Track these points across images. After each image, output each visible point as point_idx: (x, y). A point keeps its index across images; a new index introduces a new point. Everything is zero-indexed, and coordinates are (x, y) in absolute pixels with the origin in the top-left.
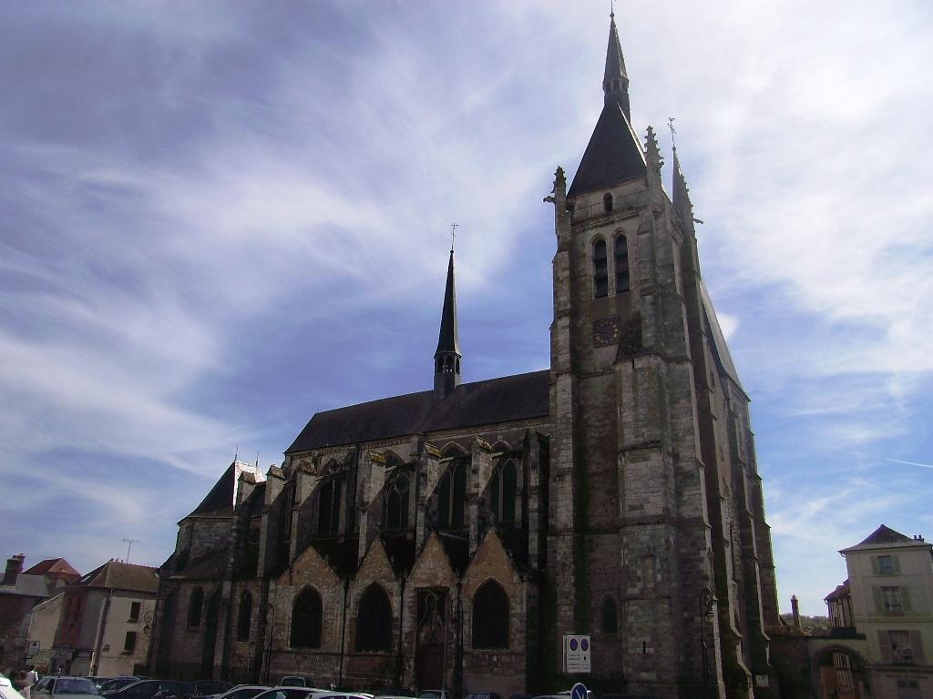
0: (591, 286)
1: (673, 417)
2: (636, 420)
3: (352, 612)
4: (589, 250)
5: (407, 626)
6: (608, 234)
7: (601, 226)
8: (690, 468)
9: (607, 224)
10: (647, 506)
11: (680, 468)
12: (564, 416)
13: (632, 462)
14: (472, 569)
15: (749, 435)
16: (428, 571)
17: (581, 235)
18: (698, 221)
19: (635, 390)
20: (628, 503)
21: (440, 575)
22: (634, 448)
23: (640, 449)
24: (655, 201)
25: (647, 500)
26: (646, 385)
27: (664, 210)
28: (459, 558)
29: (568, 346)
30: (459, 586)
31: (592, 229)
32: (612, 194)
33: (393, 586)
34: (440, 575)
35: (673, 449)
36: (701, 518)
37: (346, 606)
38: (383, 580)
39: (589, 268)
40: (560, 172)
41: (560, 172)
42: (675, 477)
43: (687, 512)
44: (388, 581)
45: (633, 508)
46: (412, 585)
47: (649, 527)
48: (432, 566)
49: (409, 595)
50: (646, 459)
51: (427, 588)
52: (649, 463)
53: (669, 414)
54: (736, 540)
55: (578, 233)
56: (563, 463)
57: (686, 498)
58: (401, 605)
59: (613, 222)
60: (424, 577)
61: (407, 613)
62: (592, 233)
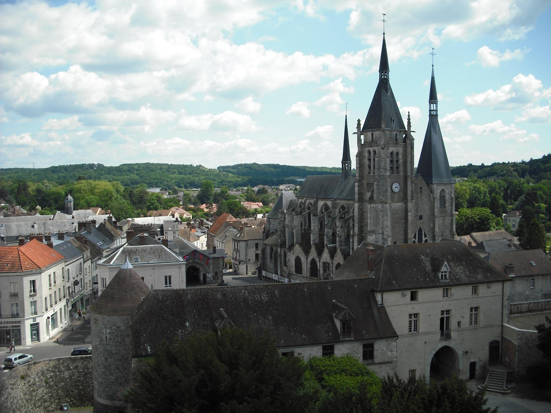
0: (367, 168)
1: (383, 221)
3: (309, 266)
4: (366, 154)
5: (321, 272)
6: (371, 149)
14: (335, 258)
28: (332, 254)
30: (332, 263)
33: (317, 260)
37: (307, 263)
39: (366, 162)
40: (359, 121)
41: (359, 121)
46: (322, 260)
48: (326, 256)
49: (321, 263)
58: (320, 266)
61: (321, 268)
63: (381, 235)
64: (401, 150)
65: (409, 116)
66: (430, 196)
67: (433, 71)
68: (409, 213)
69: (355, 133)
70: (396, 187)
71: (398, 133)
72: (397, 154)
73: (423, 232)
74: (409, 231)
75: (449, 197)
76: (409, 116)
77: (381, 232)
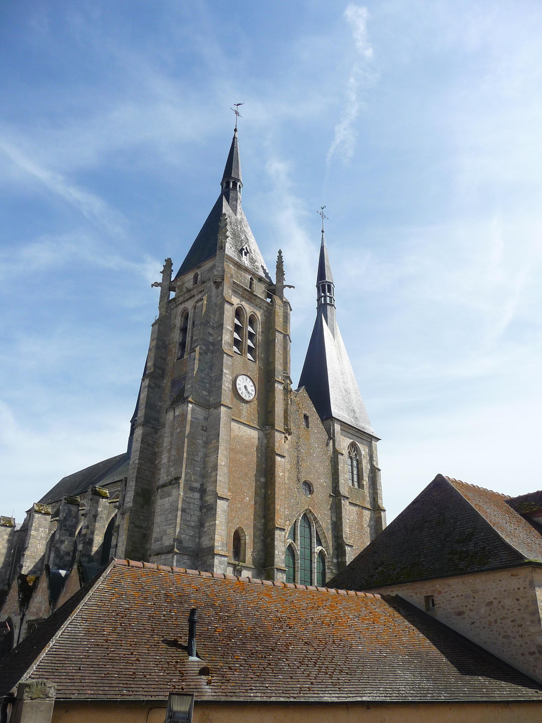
0: (176, 350)
2: (169, 462)
7: (187, 300)
8: (212, 501)
9: (191, 298)
10: (165, 538)
11: (206, 501)
12: (134, 462)
13: (161, 498)
15: (374, 471)
16: (37, 605)
17: (175, 310)
18: (290, 287)
19: (172, 435)
20: (154, 535)
21: (43, 608)
22: (164, 486)
23: (167, 486)
24: (215, 273)
25: (165, 533)
26: (178, 430)
27: (223, 280)
29: (145, 403)
31: (181, 303)
32: (199, 273)
33: (16, 620)
34: (43, 608)
35: (202, 485)
36: (212, 548)
38: (13, 615)
39: (176, 336)
40: (169, 263)
42: (201, 510)
43: (205, 542)
44: (15, 615)
45: (157, 540)
47: (163, 557)
49: (25, 626)
50: (169, 496)
51: (33, 621)
52: (171, 498)
53: (201, 454)
54: (329, 568)
55: (173, 309)
56: (128, 502)
57: (206, 529)
59: (194, 296)
60: (35, 610)
62: (181, 307)
63: (197, 495)
64: (259, 315)
65: (280, 258)
66: (327, 444)
67: (322, 239)
68: (278, 459)
69: (156, 284)
70: (247, 387)
71: (255, 281)
72: (252, 321)
73: (314, 529)
74: (277, 507)
75: (369, 467)
76: (280, 258)
77: (197, 485)
